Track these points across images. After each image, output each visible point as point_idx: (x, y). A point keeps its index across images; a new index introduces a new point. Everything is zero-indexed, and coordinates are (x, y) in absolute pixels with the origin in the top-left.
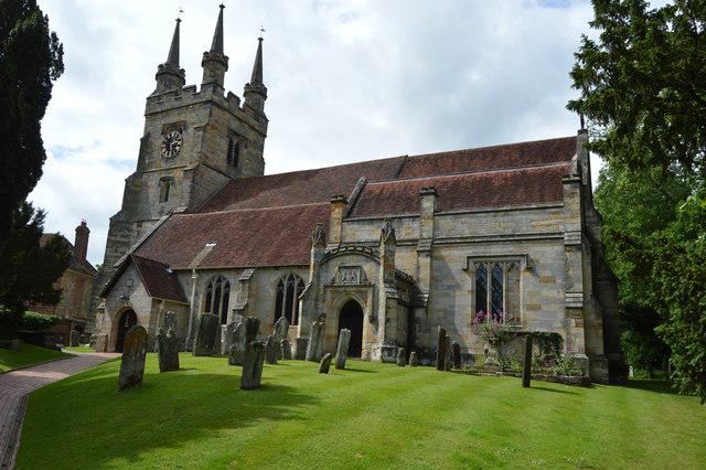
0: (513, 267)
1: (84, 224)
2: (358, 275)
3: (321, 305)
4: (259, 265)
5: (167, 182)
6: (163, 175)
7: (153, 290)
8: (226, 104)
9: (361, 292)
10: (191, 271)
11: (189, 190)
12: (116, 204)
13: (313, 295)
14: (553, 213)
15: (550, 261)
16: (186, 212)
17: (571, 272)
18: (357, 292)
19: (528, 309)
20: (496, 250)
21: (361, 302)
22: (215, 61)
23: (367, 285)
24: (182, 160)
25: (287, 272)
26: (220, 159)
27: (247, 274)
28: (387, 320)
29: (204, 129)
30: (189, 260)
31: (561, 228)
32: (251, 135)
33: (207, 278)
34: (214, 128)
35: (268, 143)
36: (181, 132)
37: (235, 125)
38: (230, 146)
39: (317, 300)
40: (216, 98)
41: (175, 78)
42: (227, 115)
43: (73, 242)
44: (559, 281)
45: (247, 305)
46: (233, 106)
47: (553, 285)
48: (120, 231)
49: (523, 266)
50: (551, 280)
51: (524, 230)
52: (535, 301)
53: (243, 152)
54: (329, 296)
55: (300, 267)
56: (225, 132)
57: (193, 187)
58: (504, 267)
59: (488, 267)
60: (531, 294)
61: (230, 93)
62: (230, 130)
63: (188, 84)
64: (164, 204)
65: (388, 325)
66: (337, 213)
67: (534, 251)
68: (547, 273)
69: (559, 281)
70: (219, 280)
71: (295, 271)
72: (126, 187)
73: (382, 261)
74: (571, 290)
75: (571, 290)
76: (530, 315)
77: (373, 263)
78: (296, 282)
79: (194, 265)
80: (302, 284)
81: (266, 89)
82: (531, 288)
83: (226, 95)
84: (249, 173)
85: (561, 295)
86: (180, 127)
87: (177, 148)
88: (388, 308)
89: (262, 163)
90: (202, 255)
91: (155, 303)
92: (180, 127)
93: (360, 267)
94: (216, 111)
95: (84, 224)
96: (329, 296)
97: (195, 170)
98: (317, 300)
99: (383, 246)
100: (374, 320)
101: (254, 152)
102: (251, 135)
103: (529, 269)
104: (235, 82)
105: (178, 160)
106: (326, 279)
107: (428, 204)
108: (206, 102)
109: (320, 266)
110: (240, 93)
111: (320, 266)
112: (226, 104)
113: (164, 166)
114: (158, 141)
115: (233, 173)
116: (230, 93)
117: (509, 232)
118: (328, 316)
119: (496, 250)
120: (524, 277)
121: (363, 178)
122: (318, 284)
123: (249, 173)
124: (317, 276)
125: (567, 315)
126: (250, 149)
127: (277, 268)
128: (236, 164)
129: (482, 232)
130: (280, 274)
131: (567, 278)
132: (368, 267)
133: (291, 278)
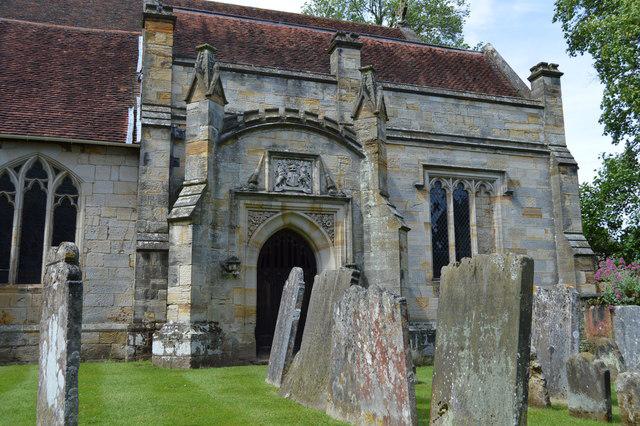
0: (485, 190)
2: (315, 173)
3: (223, 239)
9: (320, 212)
14: (532, 115)
15: (533, 186)
17: (567, 203)
18: (312, 211)
20: (462, 158)
21: (316, 237)
25: (28, 156)
31: (542, 139)
39: (214, 226)
44: (546, 216)
49: (500, 188)
50: (533, 214)
54: (243, 215)
55: (67, 147)
58: (472, 187)
59: (451, 187)
60: (514, 233)
68: (530, 203)
69: (546, 216)
74: (570, 229)
75: (570, 229)
77: (346, 154)
78: (53, 183)
80: (68, 187)
82: (512, 224)
85: (549, 236)
93: (316, 157)
96: (243, 215)
98: (214, 226)
103: (509, 194)
106: (238, 175)
107: (348, 62)
109: (221, 143)
111: (221, 143)
117: (477, 133)
118: (243, 264)
119: (462, 158)
120: (501, 206)
122: (217, 187)
124: (214, 167)
125: (577, 265)
129: (439, 127)
131: (564, 210)
133: (37, 170)
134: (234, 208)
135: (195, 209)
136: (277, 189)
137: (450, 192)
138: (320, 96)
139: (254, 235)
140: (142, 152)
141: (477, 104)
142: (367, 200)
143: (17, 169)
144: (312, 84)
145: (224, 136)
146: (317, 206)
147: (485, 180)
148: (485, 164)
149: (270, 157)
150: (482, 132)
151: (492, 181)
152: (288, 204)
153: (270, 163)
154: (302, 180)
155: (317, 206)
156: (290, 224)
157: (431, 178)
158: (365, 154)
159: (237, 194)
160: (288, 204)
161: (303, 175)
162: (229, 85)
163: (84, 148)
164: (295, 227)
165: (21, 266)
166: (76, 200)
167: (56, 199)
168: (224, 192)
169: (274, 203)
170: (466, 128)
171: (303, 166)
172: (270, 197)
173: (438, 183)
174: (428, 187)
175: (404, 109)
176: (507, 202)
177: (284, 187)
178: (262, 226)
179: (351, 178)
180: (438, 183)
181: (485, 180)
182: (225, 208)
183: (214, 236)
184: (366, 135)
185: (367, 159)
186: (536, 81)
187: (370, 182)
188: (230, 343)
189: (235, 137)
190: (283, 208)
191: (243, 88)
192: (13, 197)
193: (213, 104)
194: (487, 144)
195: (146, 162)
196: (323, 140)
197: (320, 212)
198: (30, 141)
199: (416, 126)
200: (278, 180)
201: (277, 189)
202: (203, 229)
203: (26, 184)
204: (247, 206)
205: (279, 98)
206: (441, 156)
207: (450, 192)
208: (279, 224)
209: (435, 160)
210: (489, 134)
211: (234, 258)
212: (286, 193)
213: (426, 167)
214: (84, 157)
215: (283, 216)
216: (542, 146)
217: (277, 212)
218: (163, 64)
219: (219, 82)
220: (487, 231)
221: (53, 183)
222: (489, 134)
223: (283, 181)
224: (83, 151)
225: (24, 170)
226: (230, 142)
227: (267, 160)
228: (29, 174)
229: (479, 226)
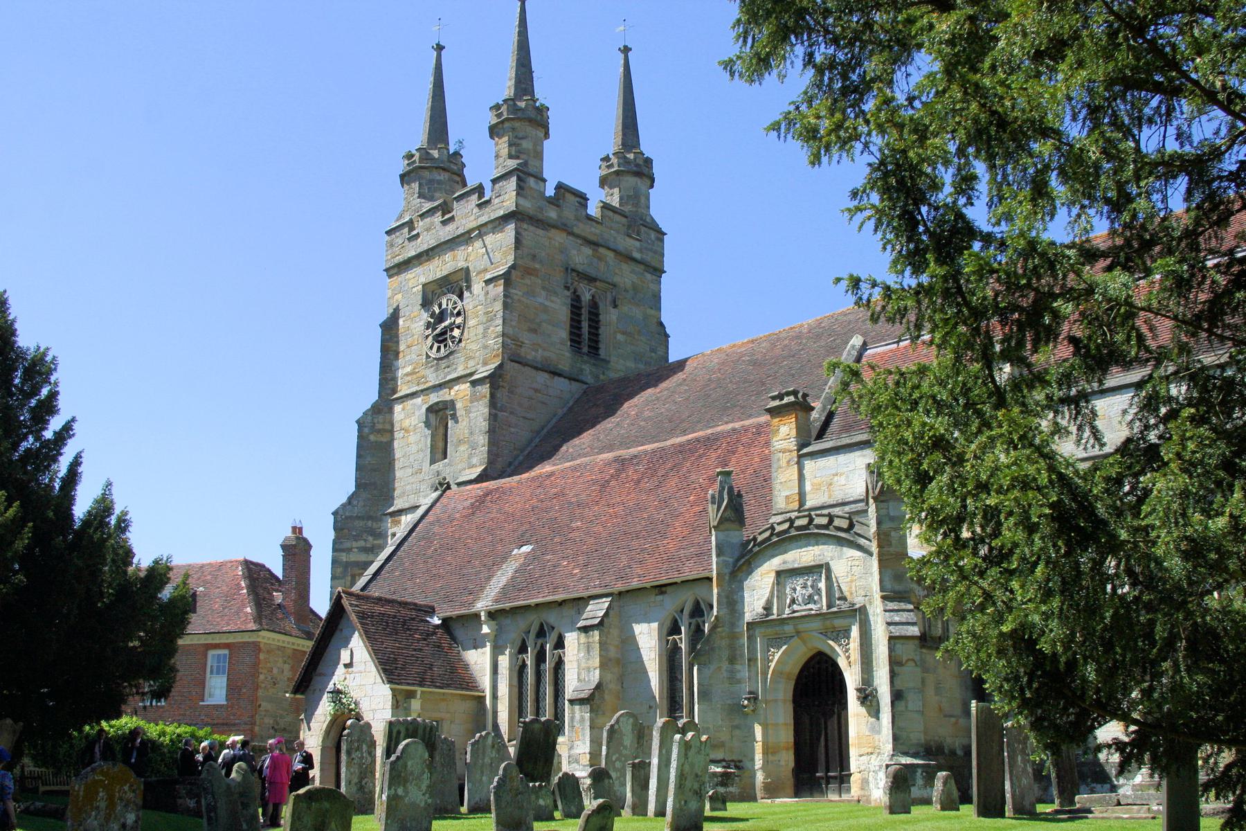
1: (297, 530)
2: (822, 585)
4: (620, 586)
5: (440, 415)
6: (434, 398)
7: (390, 669)
8: (552, 214)
10: (477, 616)
11: (484, 425)
12: (342, 484)
16: (481, 478)
22: (523, 119)
24: (469, 358)
26: (555, 342)
27: (597, 610)
28: (897, 696)
29: (507, 278)
30: (476, 593)
32: (626, 276)
33: (516, 628)
34: (529, 272)
35: (668, 284)
36: (461, 296)
37: (581, 257)
38: (576, 307)
39: (732, 660)
40: (527, 204)
41: (443, 176)
42: (559, 237)
43: (281, 578)
45: (599, 687)
46: (569, 213)
48: (356, 538)
53: (610, 317)
56: (558, 277)
57: (493, 418)
61: (560, 187)
62: (570, 270)
63: (472, 183)
64: (439, 466)
65: (901, 706)
66: (785, 433)
70: (541, 633)
72: (361, 437)
73: (874, 547)
79: (482, 605)
81: (648, 162)
83: (550, 191)
84: (631, 364)
86: (456, 283)
87: (456, 333)
88: (894, 663)
89: (662, 335)
90: (501, 578)
91: (400, 700)
92: (456, 283)
94: (531, 232)
95: (297, 530)
97: (494, 379)
99: (872, 508)
100: (868, 697)
101: (637, 312)
102: (626, 276)
104: (576, 157)
105: (459, 359)
108: (506, 218)
110: (586, 179)
112: (552, 214)
113: (433, 379)
114: (414, 324)
115: (588, 371)
116: (560, 187)
121: (857, 341)
123: (631, 364)
126: (625, 309)
128: (594, 348)
134: (751, 638)
154: (810, 596)
177: (795, 607)
183: (732, 672)
218: (788, 462)
223: (793, 601)
226: (744, 568)
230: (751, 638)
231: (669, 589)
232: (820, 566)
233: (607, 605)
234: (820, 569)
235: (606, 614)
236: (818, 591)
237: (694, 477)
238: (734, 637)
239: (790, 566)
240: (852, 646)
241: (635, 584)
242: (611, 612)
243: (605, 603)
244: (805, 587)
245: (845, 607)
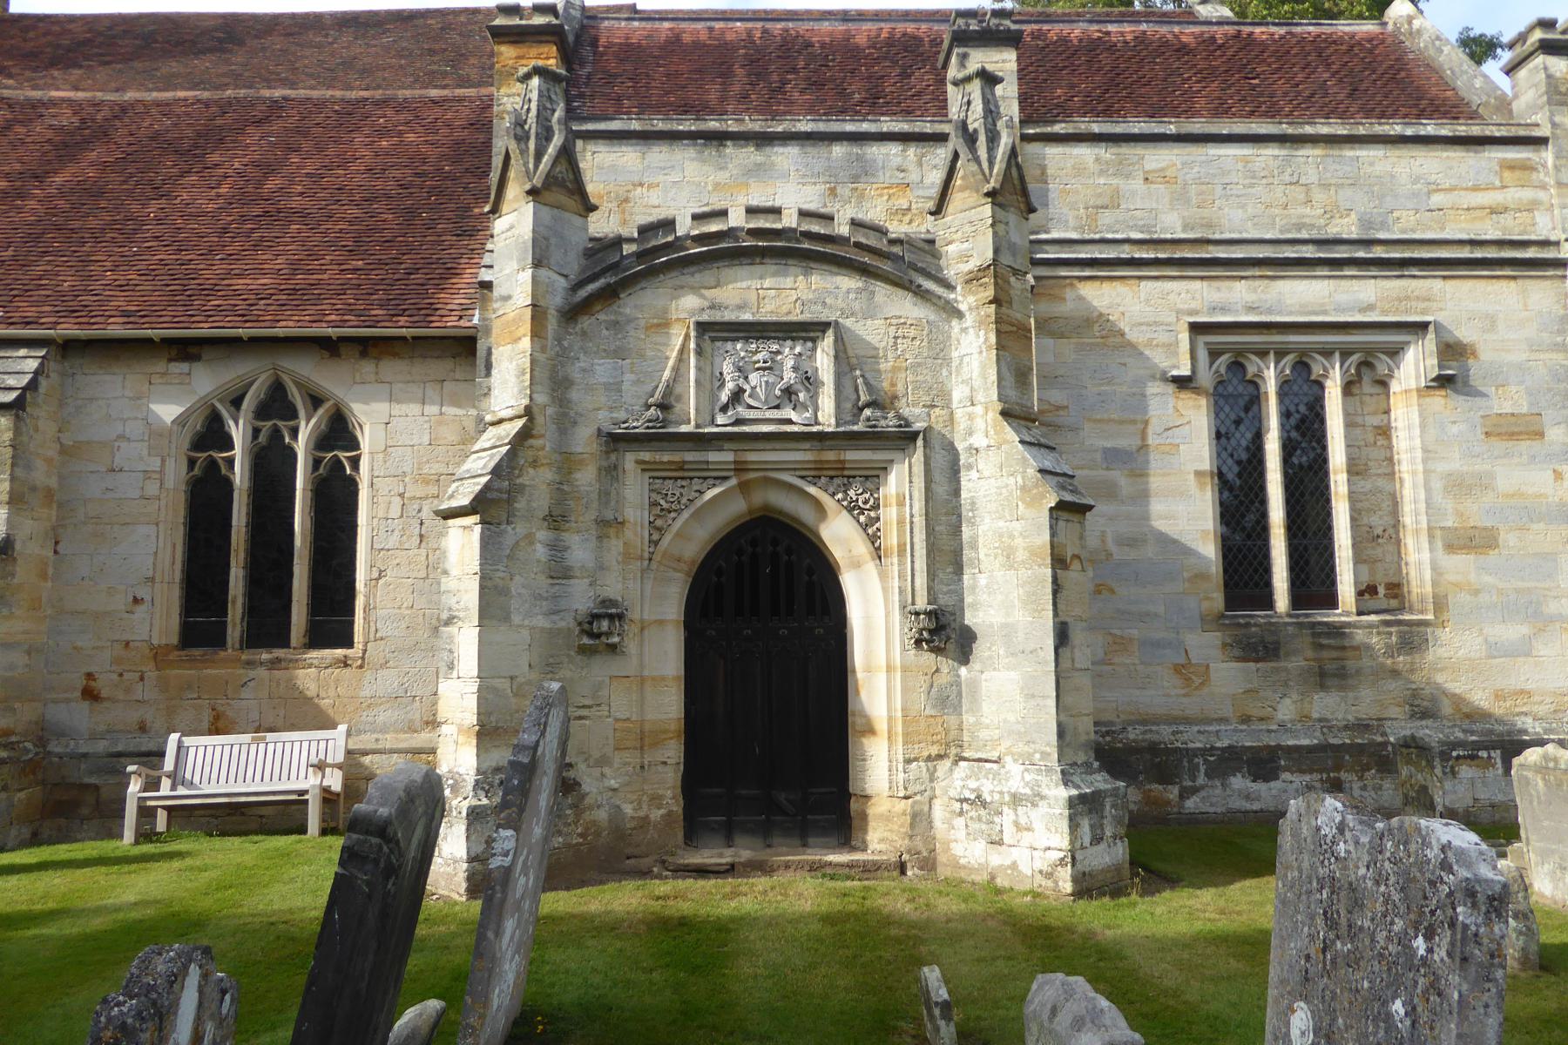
3: (580, 551)
4: (68, 330)
13: (538, 482)
14: (1511, 166)
19: (1450, 548)
23: (875, 436)
25: (255, 374)
47: (1536, 445)
50: (1517, 430)
51: (1406, 224)
52: (1477, 512)
54: (634, 491)
55: (329, 347)
60: (1459, 485)
67: (1456, 303)
68: (1509, 401)
71: (304, 370)
76: (1460, 566)
80: (339, 433)
82: (1454, 463)
98: (556, 520)
100: (943, 631)
106: (611, 396)
111: (573, 313)
117: (1347, 227)
118: (634, 614)
122: (566, 421)
124: (552, 377)
127: (186, 350)
130: (206, 381)
132: (880, 318)
134: (611, 472)
135: (487, 487)
136: (720, 419)
137: (1271, 386)
138: (914, 176)
139: (667, 538)
140: (481, 346)
141: (1349, 152)
142: (970, 433)
143: (237, 402)
144: (894, 149)
145: (583, 293)
146: (831, 456)
147: (1369, 351)
148: (1371, 308)
149: (699, 337)
150: (1365, 223)
151: (1395, 352)
152: (752, 457)
153: (699, 352)
154: (789, 392)
155: (831, 456)
156: (767, 507)
157: (1214, 354)
158: (963, 307)
159: (616, 441)
160: (752, 457)
161: (789, 376)
162: (602, 166)
163: (369, 347)
164: (780, 512)
165: (252, 610)
166: (355, 462)
167: (317, 463)
168: (584, 440)
169: (713, 456)
170: (1312, 214)
171: (789, 354)
172: (698, 440)
173: (1237, 366)
174: (1206, 378)
175: (1137, 184)
176: (1439, 401)
178: (686, 515)
179: (926, 376)
180: (1237, 366)
181: (1369, 351)
182: (586, 477)
183: (557, 548)
184: (965, 257)
185: (969, 320)
186: (1522, 73)
187: (977, 383)
188: (602, 815)
189: (610, 294)
190: (740, 468)
191: (723, 176)
192: (230, 462)
193: (546, 212)
194: (1379, 252)
195: (489, 367)
196: (847, 283)
197: (838, 476)
198: (254, 340)
199: (1172, 225)
200: (724, 397)
201: (720, 419)
202: (513, 533)
203: (256, 432)
204: (645, 467)
205: (809, 189)
206: (1239, 299)
207: (1271, 386)
208: (738, 508)
209: (1224, 310)
210: (1384, 225)
211: (612, 603)
212: (746, 429)
213: (1196, 329)
214: (367, 367)
215: (744, 487)
216: (1545, 243)
217: (725, 478)
219: (567, 155)
220: (1381, 482)
221: (306, 432)
222: (1384, 225)
223: (737, 395)
224: (364, 354)
225: (248, 404)
227: (692, 345)
228: (262, 412)
229: (1355, 469)
230: (611, 472)
231: (207, 353)
232: (823, 327)
233: (33, 365)
234: (806, 331)
235: (32, 385)
236: (810, 381)
237: (215, 158)
238: (567, 463)
239: (729, 316)
240: (889, 514)
241: (116, 330)
242: (44, 383)
243: (28, 362)
244: (770, 367)
245: (889, 423)
